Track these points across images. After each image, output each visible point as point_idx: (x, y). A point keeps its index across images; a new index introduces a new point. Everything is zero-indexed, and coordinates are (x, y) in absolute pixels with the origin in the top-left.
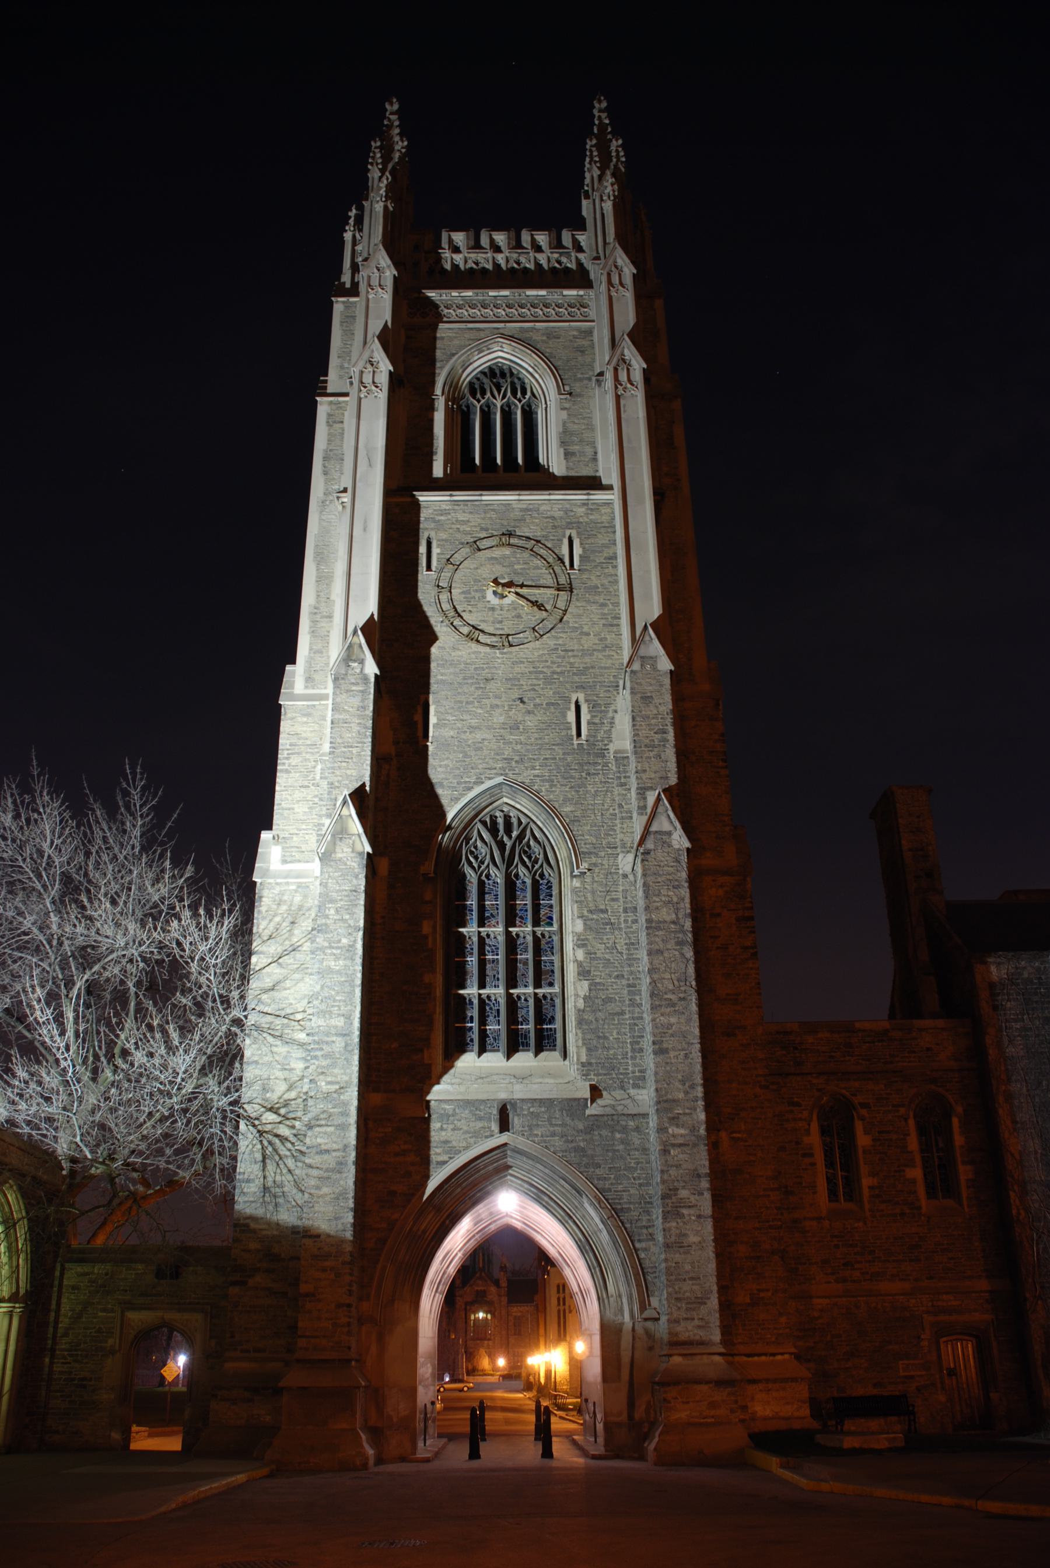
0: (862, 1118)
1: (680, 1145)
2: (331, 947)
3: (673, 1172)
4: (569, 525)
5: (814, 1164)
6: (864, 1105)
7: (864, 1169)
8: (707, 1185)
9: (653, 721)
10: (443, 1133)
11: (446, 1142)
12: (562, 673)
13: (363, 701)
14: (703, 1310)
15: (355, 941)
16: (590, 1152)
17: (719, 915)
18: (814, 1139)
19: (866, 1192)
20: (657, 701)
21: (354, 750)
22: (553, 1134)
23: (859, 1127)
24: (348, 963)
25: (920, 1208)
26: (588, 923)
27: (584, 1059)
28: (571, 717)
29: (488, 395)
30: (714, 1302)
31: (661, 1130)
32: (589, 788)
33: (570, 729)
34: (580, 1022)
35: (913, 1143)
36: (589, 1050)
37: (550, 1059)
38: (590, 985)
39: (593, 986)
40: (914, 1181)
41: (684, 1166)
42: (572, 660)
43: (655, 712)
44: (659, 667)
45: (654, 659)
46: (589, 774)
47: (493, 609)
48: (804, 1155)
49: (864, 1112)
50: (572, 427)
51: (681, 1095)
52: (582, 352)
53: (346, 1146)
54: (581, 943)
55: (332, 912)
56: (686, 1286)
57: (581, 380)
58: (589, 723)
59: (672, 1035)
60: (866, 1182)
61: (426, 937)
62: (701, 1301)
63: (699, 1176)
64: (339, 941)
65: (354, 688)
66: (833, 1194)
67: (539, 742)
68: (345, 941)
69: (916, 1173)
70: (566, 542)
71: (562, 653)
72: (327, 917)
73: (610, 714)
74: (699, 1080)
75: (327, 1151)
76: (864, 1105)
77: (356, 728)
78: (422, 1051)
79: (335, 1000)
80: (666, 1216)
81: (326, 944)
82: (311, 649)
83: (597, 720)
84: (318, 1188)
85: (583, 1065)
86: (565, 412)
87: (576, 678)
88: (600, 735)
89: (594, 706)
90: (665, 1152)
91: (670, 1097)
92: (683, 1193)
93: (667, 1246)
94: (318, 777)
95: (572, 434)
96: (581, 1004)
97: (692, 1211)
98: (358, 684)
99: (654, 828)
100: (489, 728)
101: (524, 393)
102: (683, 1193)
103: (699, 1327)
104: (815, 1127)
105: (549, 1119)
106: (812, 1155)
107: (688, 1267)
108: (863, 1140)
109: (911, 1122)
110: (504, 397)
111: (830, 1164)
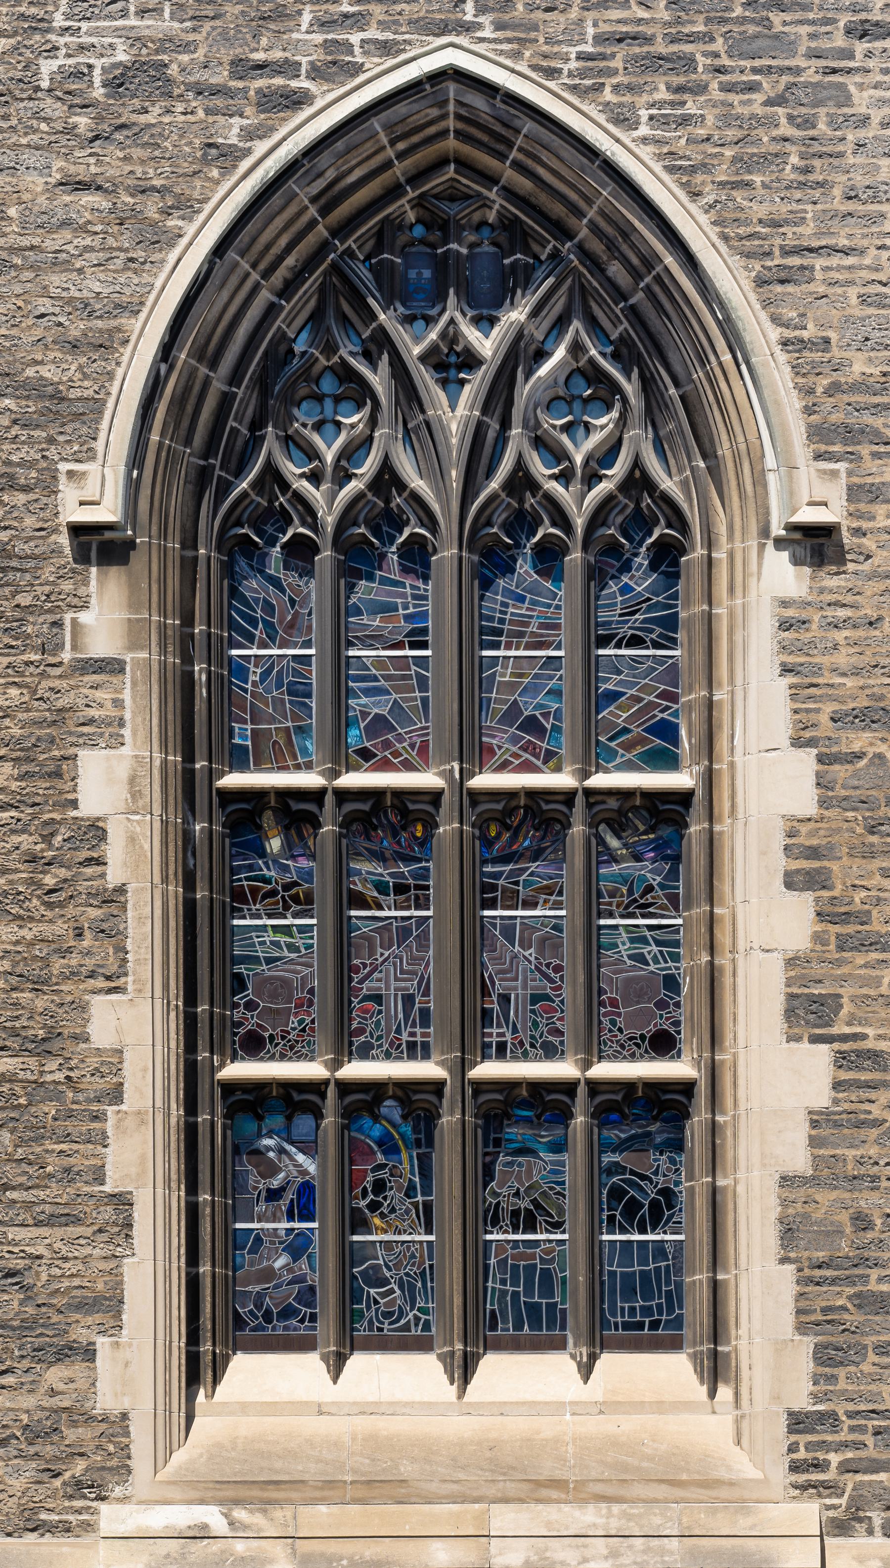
26: (840, 771)
27: (803, 1403)
36: (825, 1357)
38: (842, 1060)
61: (96, 831)
78: (89, 1354)
85: (798, 1422)
96: (800, 1161)
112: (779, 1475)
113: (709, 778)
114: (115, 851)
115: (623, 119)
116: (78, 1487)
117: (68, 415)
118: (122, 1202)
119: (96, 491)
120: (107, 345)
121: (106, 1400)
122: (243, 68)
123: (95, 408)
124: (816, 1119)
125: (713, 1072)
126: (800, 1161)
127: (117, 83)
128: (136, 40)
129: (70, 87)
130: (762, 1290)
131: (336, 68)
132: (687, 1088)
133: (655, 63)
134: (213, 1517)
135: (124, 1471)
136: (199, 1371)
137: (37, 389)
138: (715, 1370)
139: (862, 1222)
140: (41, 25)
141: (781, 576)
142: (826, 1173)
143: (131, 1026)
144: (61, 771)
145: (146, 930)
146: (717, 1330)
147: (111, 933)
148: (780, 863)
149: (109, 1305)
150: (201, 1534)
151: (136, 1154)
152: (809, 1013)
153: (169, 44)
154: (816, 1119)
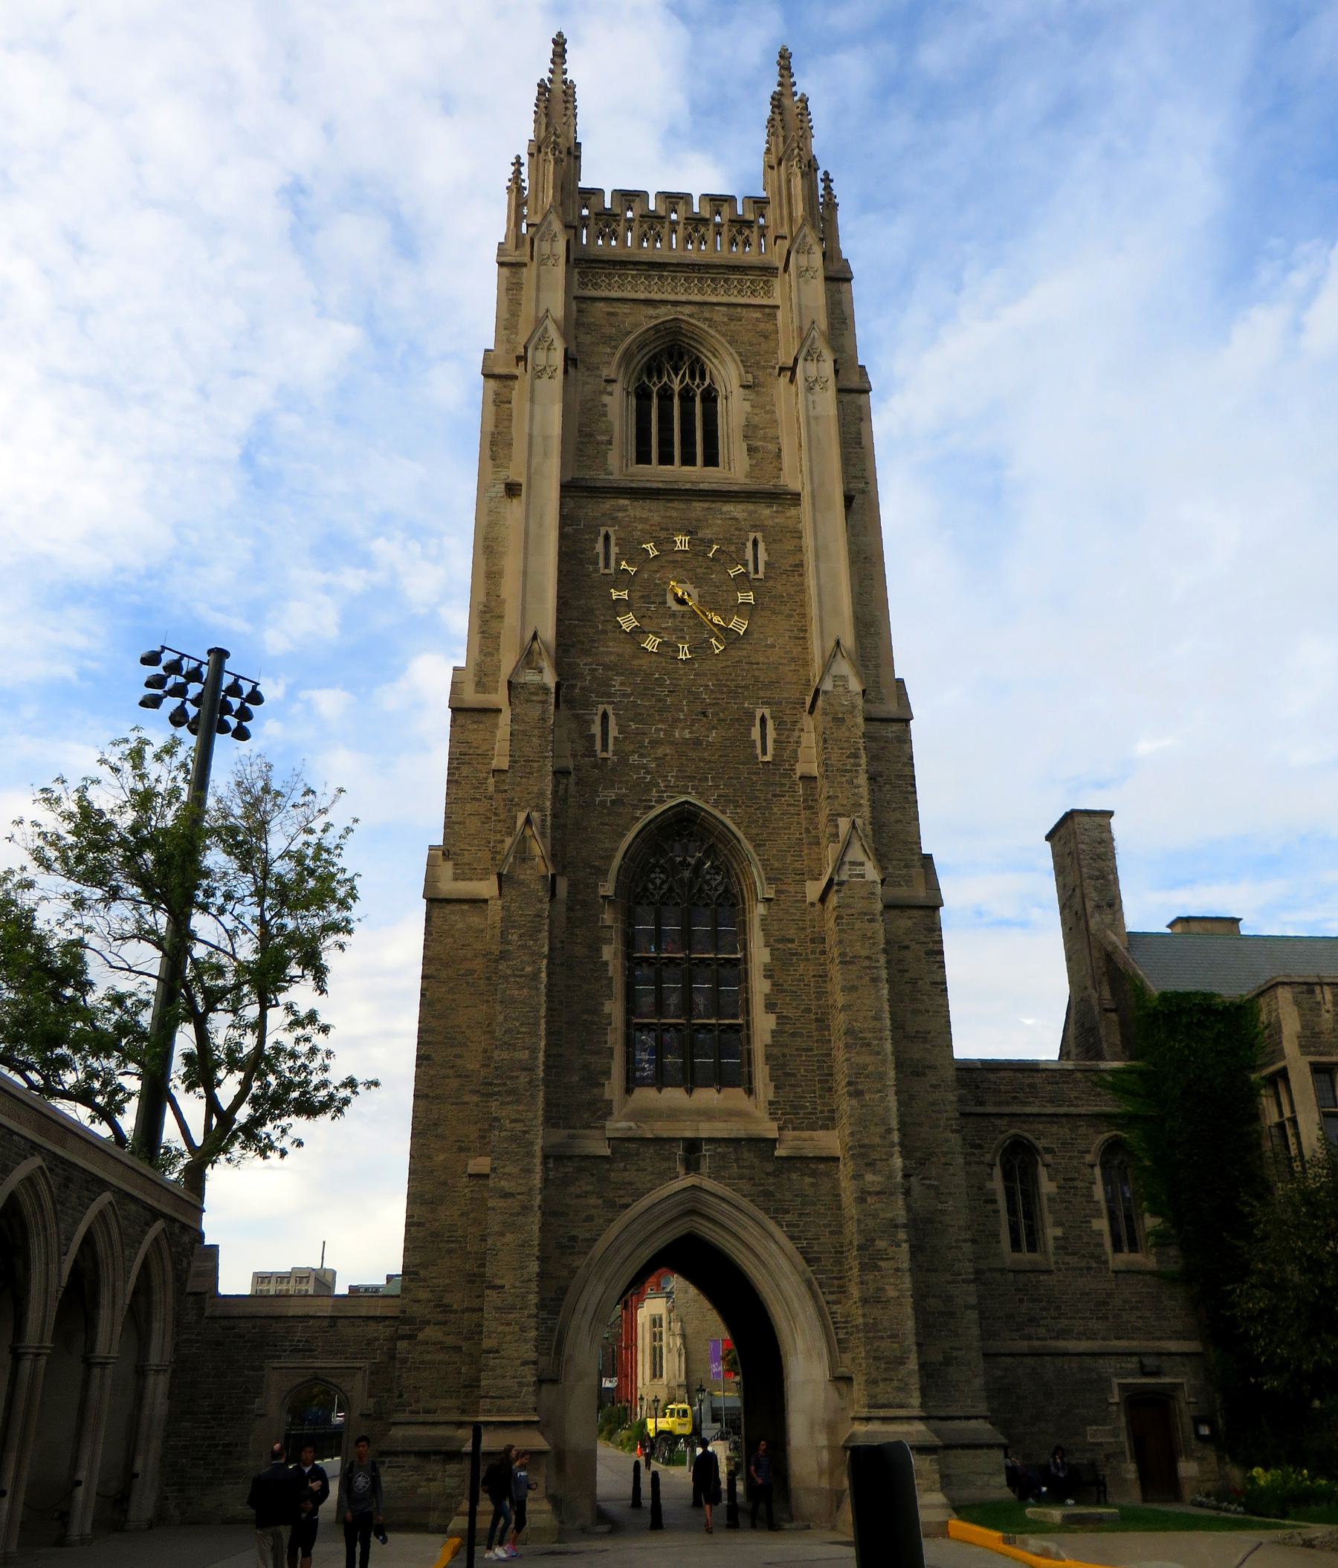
0: (1047, 1166)
1: (878, 1193)
2: (516, 976)
3: (871, 1222)
4: (755, 527)
5: (996, 1212)
6: (1049, 1150)
7: (1048, 1218)
8: (905, 1237)
9: (845, 745)
10: (627, 1174)
11: (631, 1184)
12: (746, 687)
13: (544, 712)
14: (903, 1371)
15: (539, 970)
16: (778, 1196)
17: (907, 947)
18: (997, 1184)
19: (1051, 1243)
20: (849, 723)
21: (535, 765)
22: (741, 1177)
23: (1043, 1173)
24: (533, 992)
25: (1106, 1262)
27: (771, 1097)
28: (756, 733)
29: (665, 379)
30: (913, 1364)
31: (857, 1176)
32: (775, 810)
33: (754, 747)
34: (768, 1057)
35: (1099, 1192)
36: (777, 1087)
37: (734, 1097)
38: (778, 1018)
39: (782, 1019)
40: (1100, 1234)
41: (881, 1215)
42: (756, 673)
43: (847, 734)
44: (851, 688)
45: (844, 678)
46: (774, 796)
47: (674, 615)
48: (987, 1201)
49: (1048, 1158)
50: (756, 420)
51: (877, 1140)
52: (766, 337)
53: (531, 1190)
54: (769, 973)
55: (515, 937)
56: (885, 1344)
57: (764, 367)
58: (775, 741)
59: (867, 1076)
60: (1052, 1233)
61: (606, 963)
62: (901, 1361)
63: (896, 1226)
64: (523, 969)
65: (535, 698)
66: (1016, 1245)
67: (723, 759)
68: (529, 969)
69: (1102, 1224)
70: (749, 545)
71: (747, 667)
72: (509, 943)
73: (796, 733)
74: (894, 1124)
75: (512, 1195)
76: (1049, 1150)
77: (536, 741)
79: (519, 1033)
80: (863, 1267)
81: (509, 972)
82: (481, 651)
83: (783, 738)
84: (502, 1234)
85: (771, 1103)
86: (748, 403)
87: (762, 694)
88: (786, 755)
89: (780, 725)
90: (861, 1200)
91: (866, 1141)
92: (881, 1244)
93: (865, 1301)
94: (491, 789)
95: (756, 426)
96: (769, 1041)
97: (891, 1263)
98: (537, 694)
99: (847, 859)
100: (672, 743)
101: (703, 378)
102: (881, 1244)
103: (899, 1389)
104: (997, 1172)
105: (737, 1160)
106: (995, 1201)
107: (886, 1324)
108: (1047, 1187)
109: (1097, 1171)
110: (682, 382)
111: (1012, 1211)
112: (767, 1116)
113: (745, 955)
114: (611, 968)
115: (723, 812)
116: (600, 1118)
117: (602, 873)
118: (611, 1049)
119: (608, 889)
120: (610, 858)
121: (607, 1096)
122: (640, 801)
123: (605, 873)
124: (773, 1031)
125: (748, 1022)
126: (769, 1041)
127: (613, 802)
128: (617, 794)
129: (603, 803)
130: (761, 1071)
131: (660, 801)
132: (740, 1025)
133: (730, 801)
134: (632, 1124)
135: (610, 1113)
136: (629, 1091)
137: (593, 867)
138: (750, 1091)
139: (784, 1055)
140: (596, 791)
141: (761, 909)
142: (775, 1043)
143: (614, 1008)
144: (599, 950)
145: (618, 987)
146: (750, 1082)
147: (609, 986)
148: (762, 973)
149: (607, 1074)
150: (630, 1129)
151: (615, 1038)
152: (770, 1007)
153: (626, 795)
154: (773, 1031)
